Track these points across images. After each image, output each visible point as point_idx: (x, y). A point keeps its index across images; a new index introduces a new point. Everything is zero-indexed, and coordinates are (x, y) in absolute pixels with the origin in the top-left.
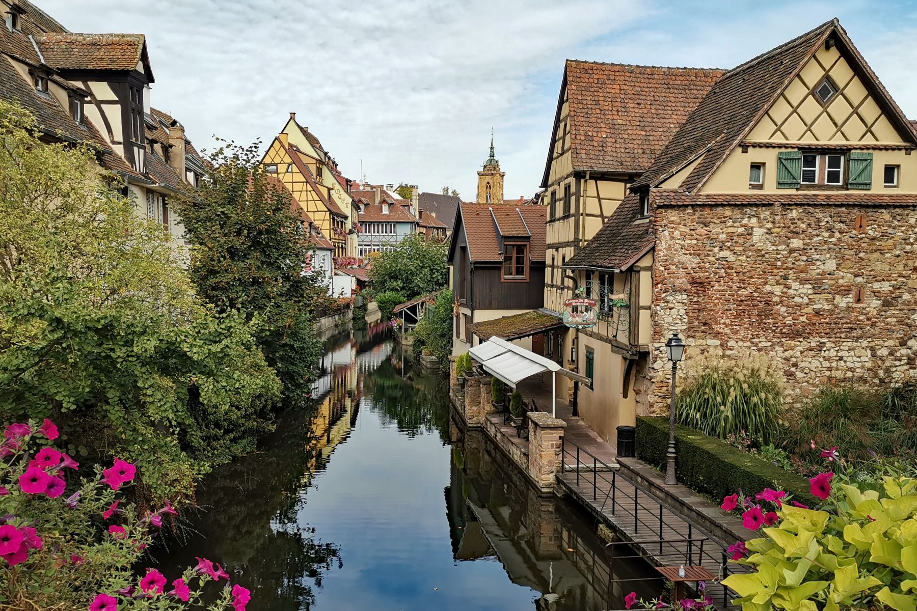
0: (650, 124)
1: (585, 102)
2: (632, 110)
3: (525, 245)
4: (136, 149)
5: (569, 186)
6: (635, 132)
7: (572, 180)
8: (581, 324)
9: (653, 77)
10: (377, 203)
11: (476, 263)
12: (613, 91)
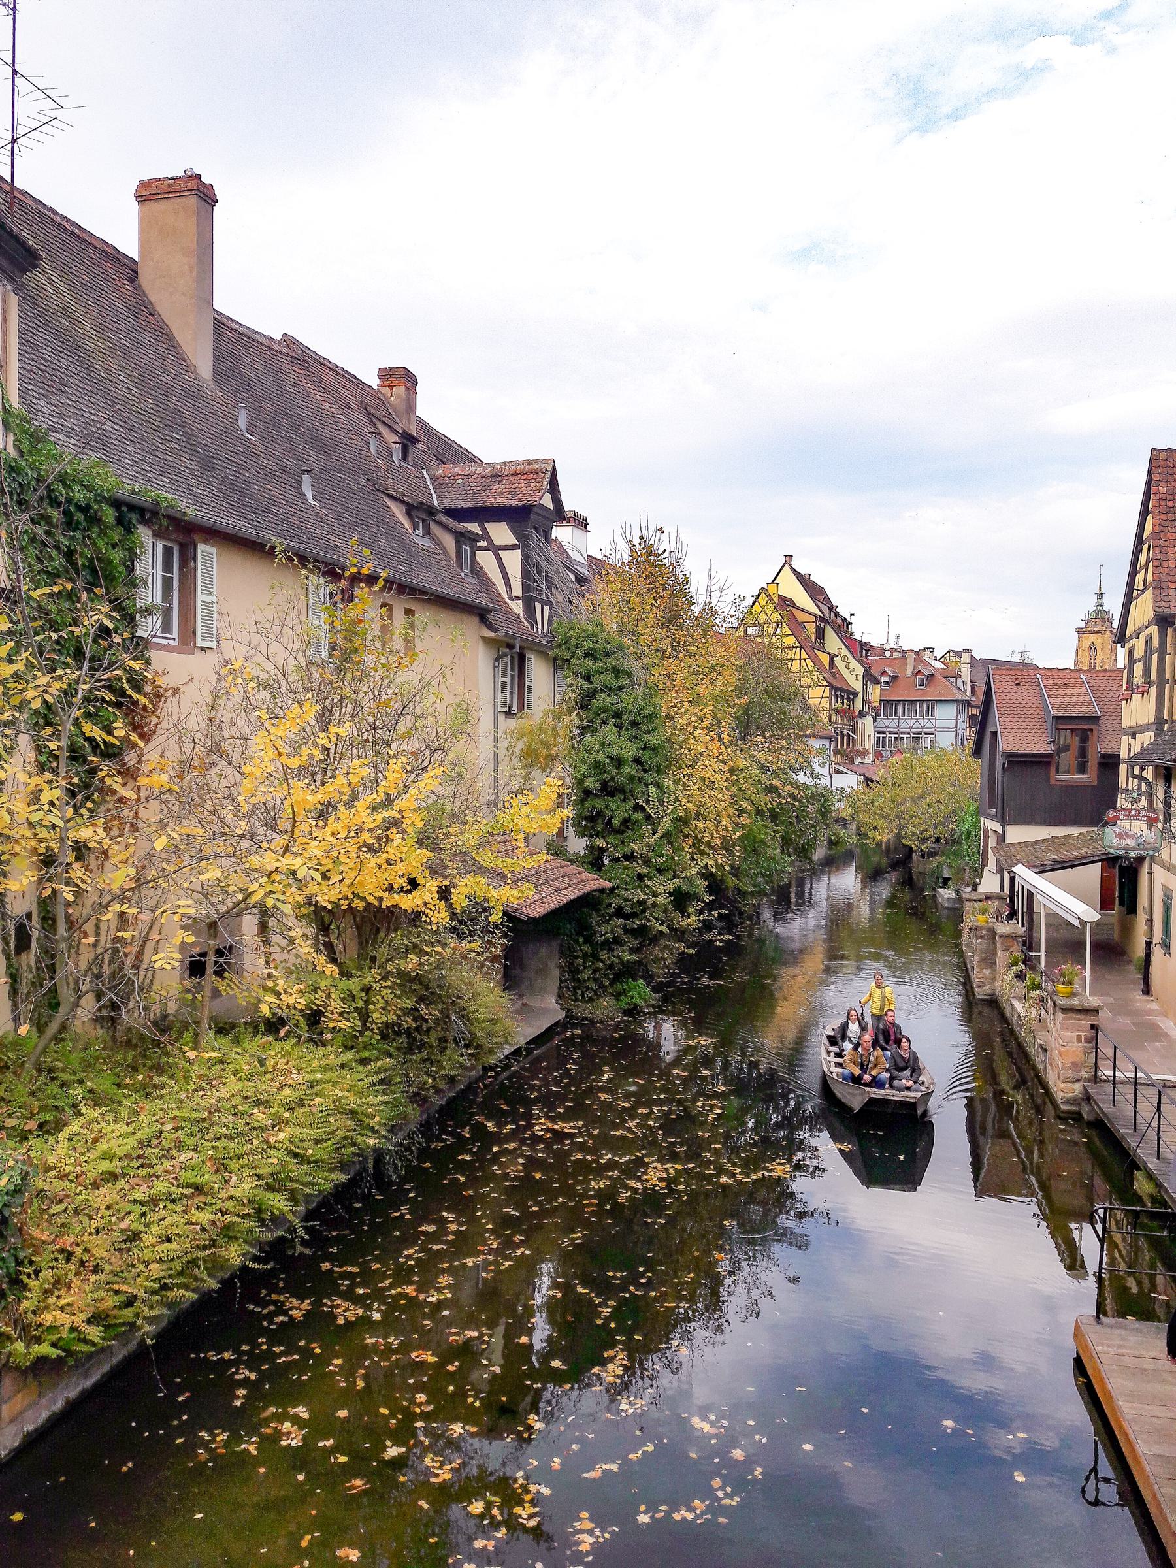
4: (538, 606)
7: (1154, 630)
8: (1133, 849)
10: (909, 674)
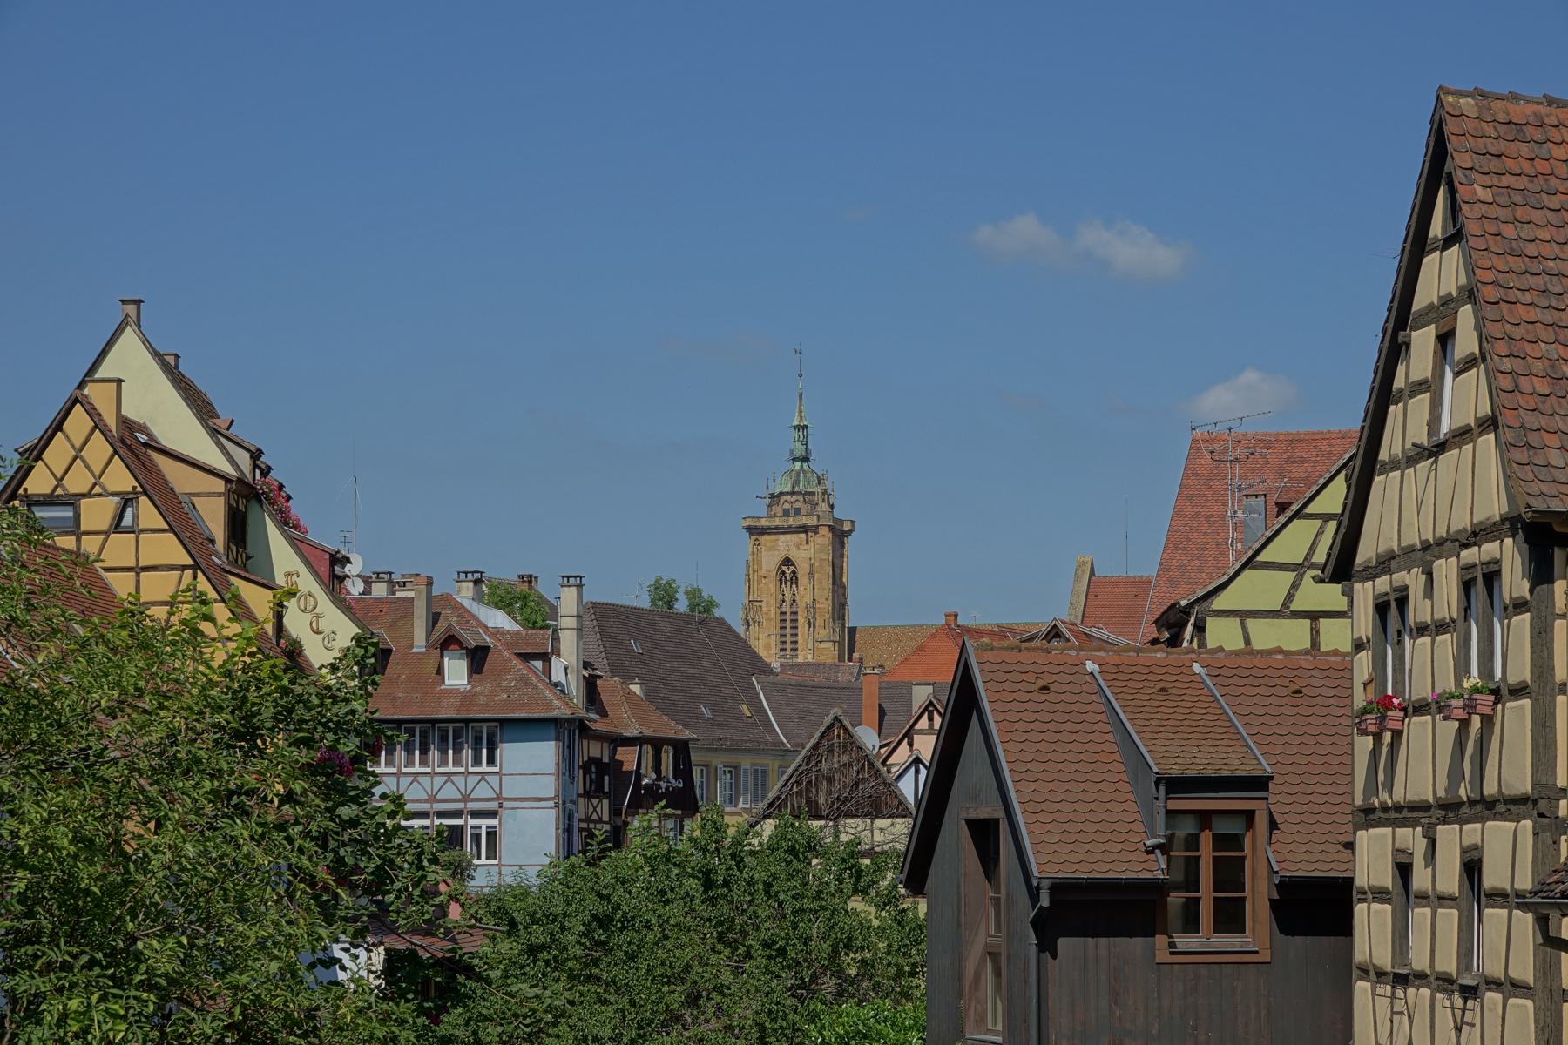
1: (1531, 249)
3: (1249, 816)
5: (1498, 573)
11: (1060, 889)
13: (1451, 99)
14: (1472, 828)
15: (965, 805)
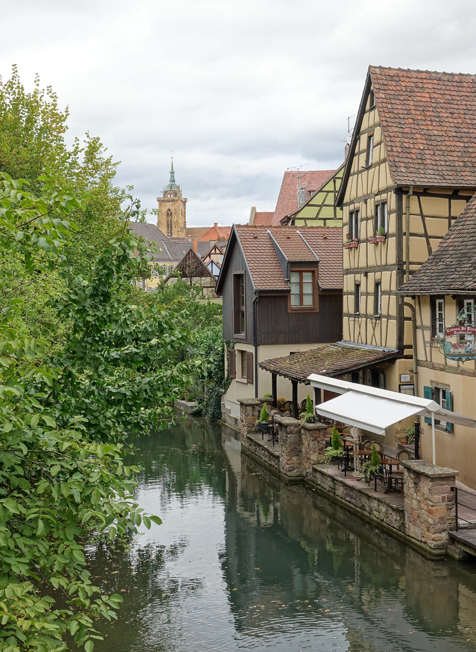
0: (467, 135)
1: (396, 111)
2: (446, 120)
5: (386, 202)
6: (452, 144)
7: (392, 198)
8: (464, 355)
9: (462, 85)
11: (261, 292)
12: (424, 100)
13: (373, 69)
14: (378, 274)
15: (234, 270)
